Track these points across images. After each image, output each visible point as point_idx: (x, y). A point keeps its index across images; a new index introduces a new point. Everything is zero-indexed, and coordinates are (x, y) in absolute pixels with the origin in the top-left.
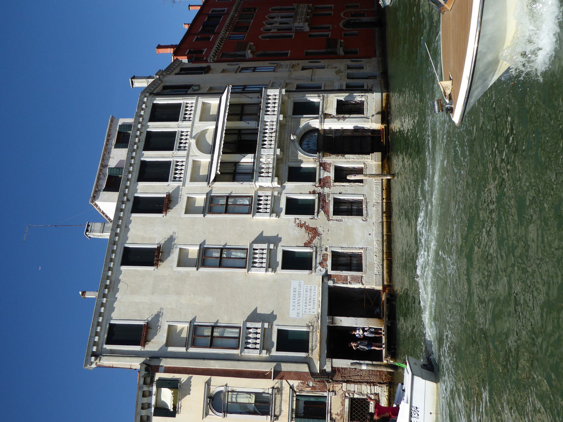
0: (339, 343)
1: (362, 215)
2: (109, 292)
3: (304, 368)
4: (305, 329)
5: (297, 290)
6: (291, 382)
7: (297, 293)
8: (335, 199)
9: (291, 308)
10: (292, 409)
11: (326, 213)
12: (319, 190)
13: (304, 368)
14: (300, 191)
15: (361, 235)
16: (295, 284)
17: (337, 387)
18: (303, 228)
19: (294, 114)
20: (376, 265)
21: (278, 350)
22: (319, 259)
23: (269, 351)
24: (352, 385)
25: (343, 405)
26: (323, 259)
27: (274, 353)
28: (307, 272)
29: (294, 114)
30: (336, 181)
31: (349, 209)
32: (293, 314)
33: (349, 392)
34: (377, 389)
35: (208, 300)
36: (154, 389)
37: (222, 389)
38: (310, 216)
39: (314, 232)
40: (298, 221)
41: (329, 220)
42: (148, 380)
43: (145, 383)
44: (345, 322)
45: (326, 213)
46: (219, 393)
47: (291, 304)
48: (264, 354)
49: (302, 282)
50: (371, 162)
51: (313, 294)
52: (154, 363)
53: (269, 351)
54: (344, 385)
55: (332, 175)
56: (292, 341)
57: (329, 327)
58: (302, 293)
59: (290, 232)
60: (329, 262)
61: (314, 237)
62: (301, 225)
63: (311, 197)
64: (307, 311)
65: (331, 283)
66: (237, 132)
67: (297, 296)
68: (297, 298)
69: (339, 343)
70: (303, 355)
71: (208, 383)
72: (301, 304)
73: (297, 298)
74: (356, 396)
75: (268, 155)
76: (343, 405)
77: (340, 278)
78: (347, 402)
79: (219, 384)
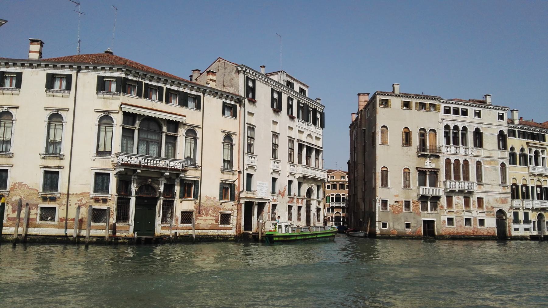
11: (289, 202)
13: (241, 190)
17: (235, 207)
22: (275, 198)
23: (247, 169)
25: (229, 210)
27: (246, 172)
34: (234, 229)
36: (233, 103)
37: (234, 142)
39: (283, 195)
45: (289, 202)
46: (231, 140)
48: (246, 167)
54: (236, 211)
55: (300, 205)
60: (274, 203)
70: (245, 188)
71: (235, 135)
74: (232, 217)
75: (310, 173)
76: (229, 210)
78: (229, 212)
79: (235, 139)
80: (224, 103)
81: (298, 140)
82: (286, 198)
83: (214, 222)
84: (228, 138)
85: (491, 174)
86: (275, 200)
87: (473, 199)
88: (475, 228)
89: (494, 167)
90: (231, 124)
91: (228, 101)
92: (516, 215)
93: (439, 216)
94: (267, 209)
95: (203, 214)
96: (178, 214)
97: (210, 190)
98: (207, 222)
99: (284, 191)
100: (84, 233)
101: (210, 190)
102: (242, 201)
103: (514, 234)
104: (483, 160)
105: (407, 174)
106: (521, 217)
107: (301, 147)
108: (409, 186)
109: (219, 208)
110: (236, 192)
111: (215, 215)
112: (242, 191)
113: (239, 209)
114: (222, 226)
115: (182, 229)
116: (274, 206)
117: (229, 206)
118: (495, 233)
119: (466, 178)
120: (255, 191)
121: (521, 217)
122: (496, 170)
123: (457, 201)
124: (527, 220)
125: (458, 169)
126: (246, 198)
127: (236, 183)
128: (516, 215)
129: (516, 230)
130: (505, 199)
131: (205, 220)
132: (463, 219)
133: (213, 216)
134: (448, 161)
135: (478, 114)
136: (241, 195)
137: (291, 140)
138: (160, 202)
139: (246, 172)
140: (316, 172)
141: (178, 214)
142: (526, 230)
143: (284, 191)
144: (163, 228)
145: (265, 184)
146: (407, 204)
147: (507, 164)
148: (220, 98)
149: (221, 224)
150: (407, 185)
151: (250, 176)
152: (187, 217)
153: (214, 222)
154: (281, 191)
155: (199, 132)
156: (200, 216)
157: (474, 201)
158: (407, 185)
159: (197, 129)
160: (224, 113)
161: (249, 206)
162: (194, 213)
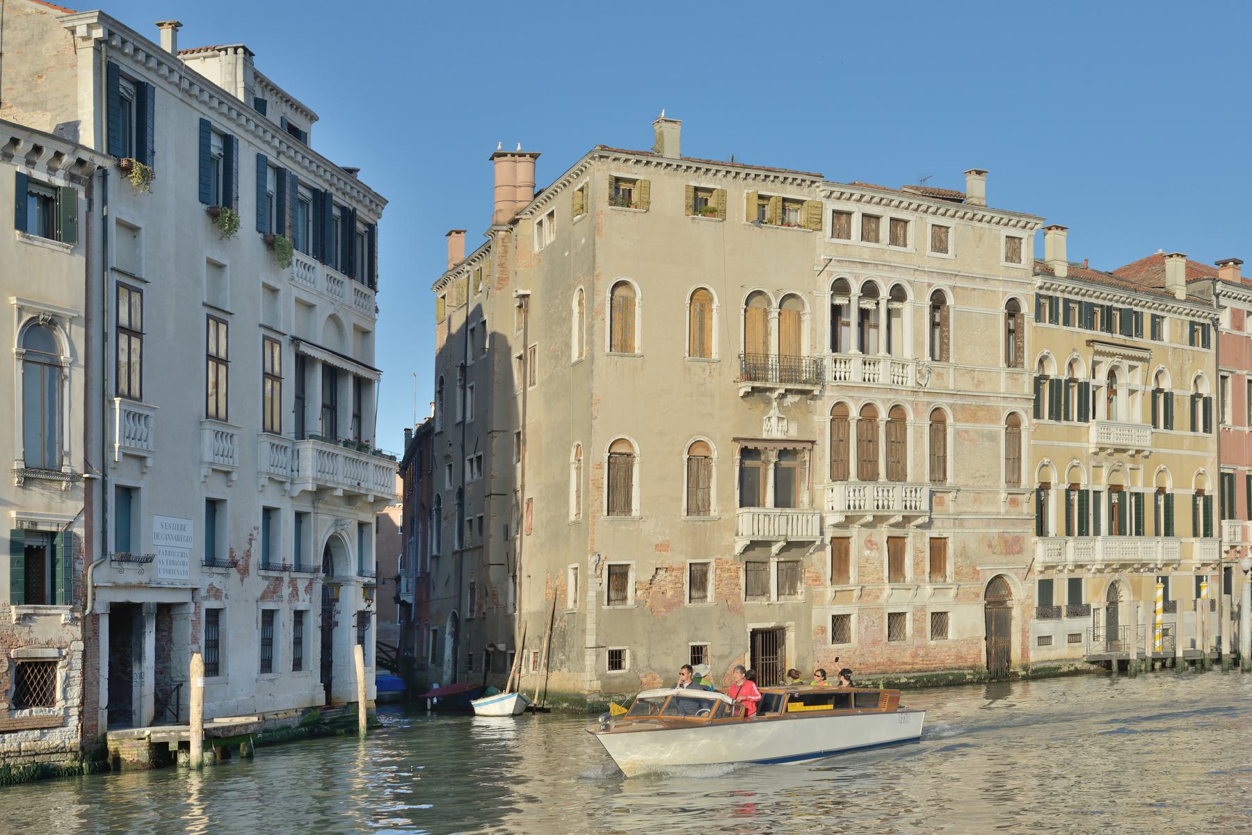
10: (35, 524)
22: (217, 581)
24: (80, 666)
32: (158, 521)
39: (245, 572)
40: (255, 532)
55: (301, 606)
57: (140, 605)
60: (213, 604)
80: (23, 182)
81: (295, 340)
82: (257, 582)
84: (38, 332)
85: (975, 456)
86: (215, 593)
87: (916, 546)
88: (916, 650)
89: (989, 427)
91: (40, 175)
92: (1046, 588)
93: (804, 612)
94: (190, 629)
99: (248, 554)
102: (102, 609)
103: (1038, 656)
104: (952, 406)
105: (697, 464)
106: (1061, 597)
107: (303, 362)
108: (707, 510)
113: (89, 639)
116: (213, 616)
118: (979, 655)
119: (897, 473)
120: (149, 559)
121: (1061, 597)
122: (992, 437)
123: (867, 552)
124: (1077, 607)
125: (871, 444)
126: (117, 587)
127: (79, 531)
128: (1046, 588)
129: (1044, 640)
130: (1018, 539)
132: (881, 617)
134: (839, 414)
135: (940, 244)
137: (271, 337)
139: (113, 480)
140: (361, 469)
142: (1074, 638)
145: (183, 528)
146: (698, 579)
147: (1027, 420)
150: (698, 505)
151: (127, 494)
154: (239, 555)
157: (918, 551)
158: (698, 505)
160: (21, 223)
161: (125, 619)
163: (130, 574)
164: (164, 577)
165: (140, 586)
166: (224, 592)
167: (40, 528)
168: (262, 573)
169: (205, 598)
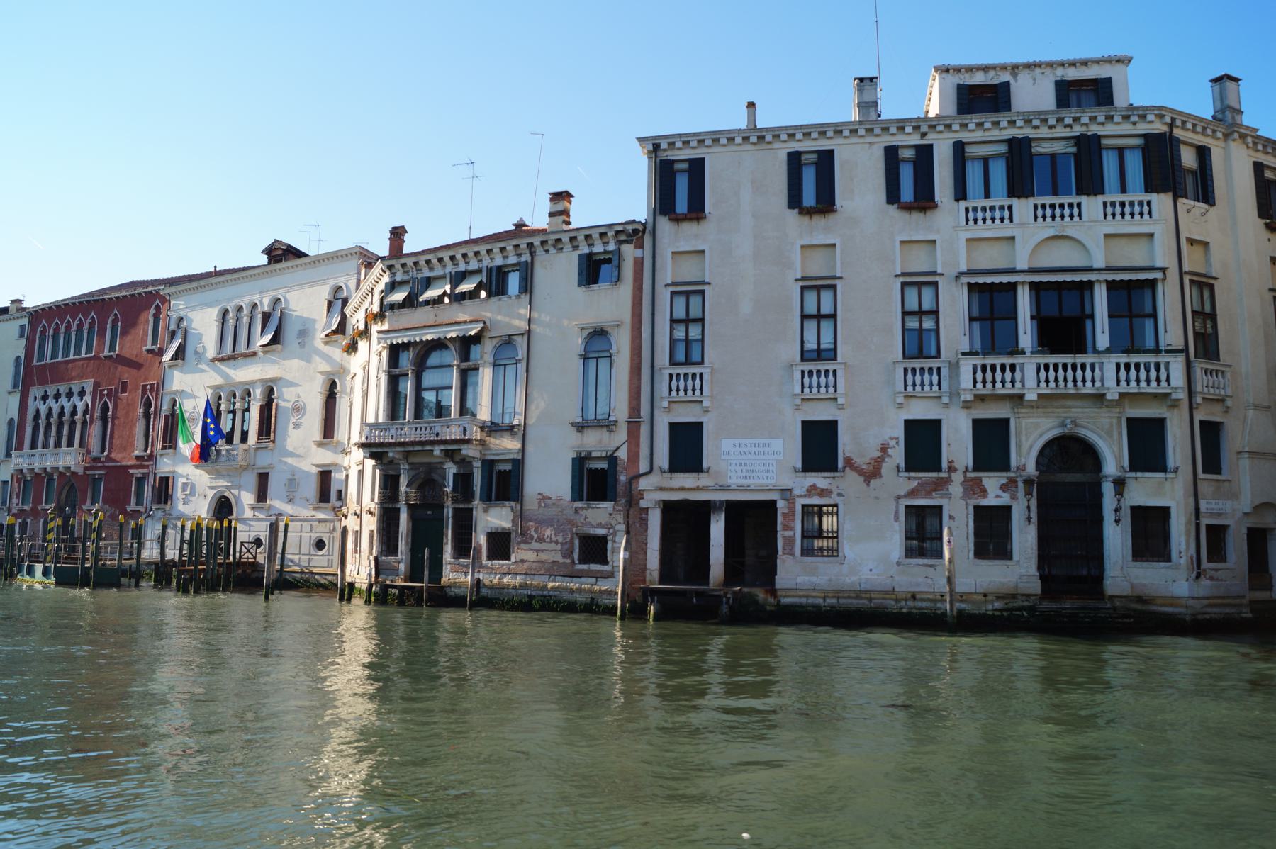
0: (685, 521)
1: (907, 556)
2: (754, 144)
3: (643, 466)
4: (705, 465)
5: (766, 449)
6: (625, 447)
7: (761, 449)
8: (940, 507)
9: (737, 441)
12: (958, 478)
13: (643, 466)
14: (957, 444)
15: (869, 553)
16: (777, 444)
17: (620, 518)
18: (879, 454)
19: (1129, 419)
20: (814, 579)
21: (673, 426)
25: (600, 525)
26: (823, 490)
28: (799, 465)
29: (1129, 419)
30: (977, 508)
31: (922, 532)
32: (726, 444)
33: (614, 534)
35: (746, 308)
37: (614, 348)
38: (902, 465)
39: (871, 473)
40: (892, 443)
41: (899, 497)
42: (623, 237)
43: (618, 232)
44: (718, 529)
45: (912, 493)
47: (744, 441)
49: (781, 457)
50: (1020, 570)
51: (760, 475)
52: (647, 240)
53: (668, 410)
54: (623, 527)
55: (990, 501)
56: (687, 447)
58: (761, 457)
59: (871, 428)
61: (860, 472)
62: (884, 449)
63: (945, 465)
64: (733, 468)
65: (781, 504)
66: (1088, 311)
67: (757, 450)
68: (753, 450)
69: (685, 521)
72: (744, 456)
73: (753, 450)
74: (609, 546)
76: (600, 525)
77: (790, 515)
79: (621, 342)
82: (897, 483)
83: (559, 558)
90: (610, 304)
91: (598, 248)
95: (532, 537)
96: (481, 539)
97: (549, 478)
98: (543, 556)
99: (879, 461)
100: (360, 570)
101: (549, 478)
109: (570, 522)
110: (622, 478)
111: (560, 539)
112: (651, 471)
114: (585, 567)
115: (492, 571)
117: (601, 516)
126: (662, 489)
127: (622, 454)
131: (537, 551)
133: (557, 543)
136: (643, 484)
138: (449, 512)
141: (481, 539)
143: (879, 461)
144: (453, 570)
148: (576, 248)
149: (582, 561)
152: (500, 545)
153: (559, 558)
155: (521, 343)
156: (526, 543)
159: (518, 339)
162: (513, 536)
163: (686, 480)
164: (733, 481)
165: (697, 489)
166: (835, 491)
167: (594, 455)
168: (906, 474)
169: (801, 496)
